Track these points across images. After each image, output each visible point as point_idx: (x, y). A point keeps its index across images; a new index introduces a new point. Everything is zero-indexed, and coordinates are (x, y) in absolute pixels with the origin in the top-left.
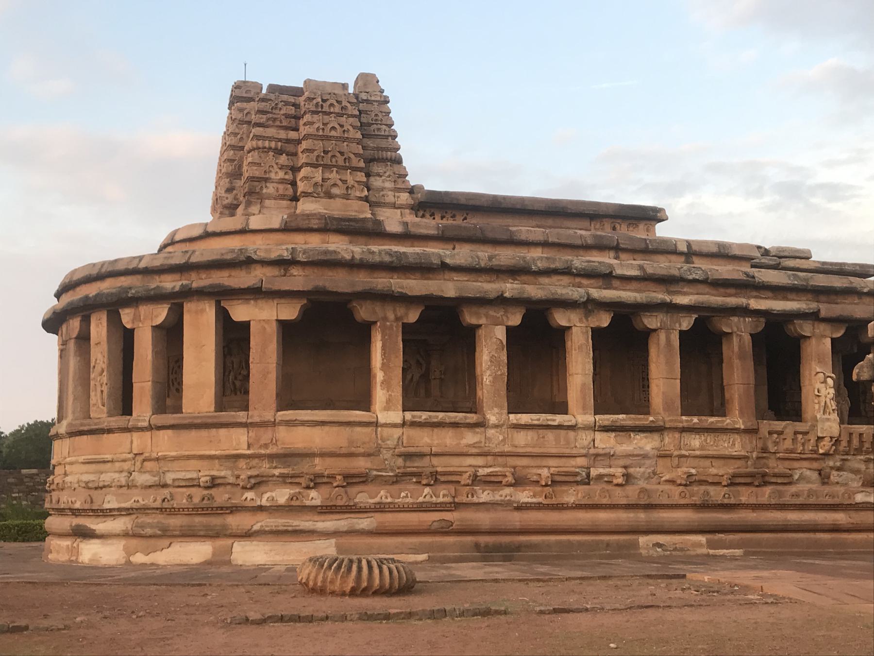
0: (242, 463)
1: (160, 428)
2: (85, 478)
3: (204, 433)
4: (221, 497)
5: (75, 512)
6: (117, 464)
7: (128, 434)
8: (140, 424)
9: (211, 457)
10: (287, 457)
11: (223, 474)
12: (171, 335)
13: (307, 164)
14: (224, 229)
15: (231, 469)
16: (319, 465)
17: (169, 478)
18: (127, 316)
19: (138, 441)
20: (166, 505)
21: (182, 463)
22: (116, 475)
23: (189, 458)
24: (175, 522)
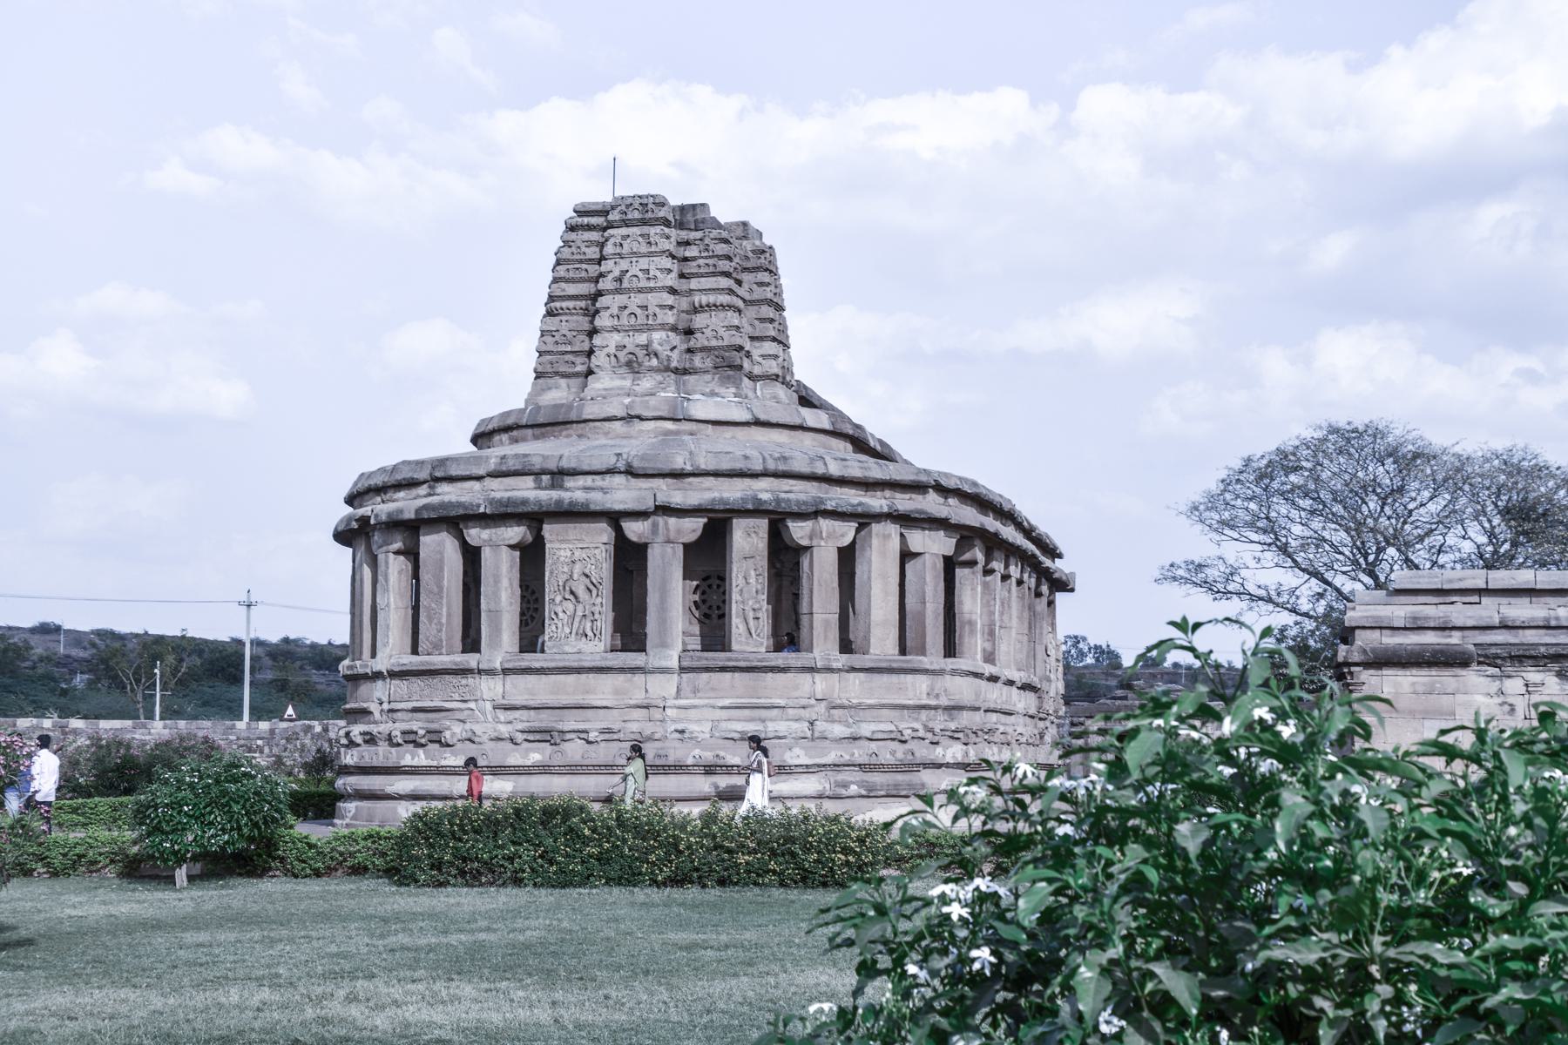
0: (924, 714)
1: (853, 669)
2: (739, 727)
3: (894, 678)
4: (923, 752)
5: (710, 770)
6: (790, 711)
7: (808, 676)
8: (835, 665)
9: (904, 707)
10: (953, 709)
11: (916, 725)
12: (847, 556)
13: (774, 339)
14: (781, 421)
15: (917, 720)
16: (966, 719)
17: (866, 729)
18: (799, 531)
19: (821, 684)
20: (874, 760)
21: (875, 712)
22: (795, 726)
23: (883, 706)
24: (877, 778)
